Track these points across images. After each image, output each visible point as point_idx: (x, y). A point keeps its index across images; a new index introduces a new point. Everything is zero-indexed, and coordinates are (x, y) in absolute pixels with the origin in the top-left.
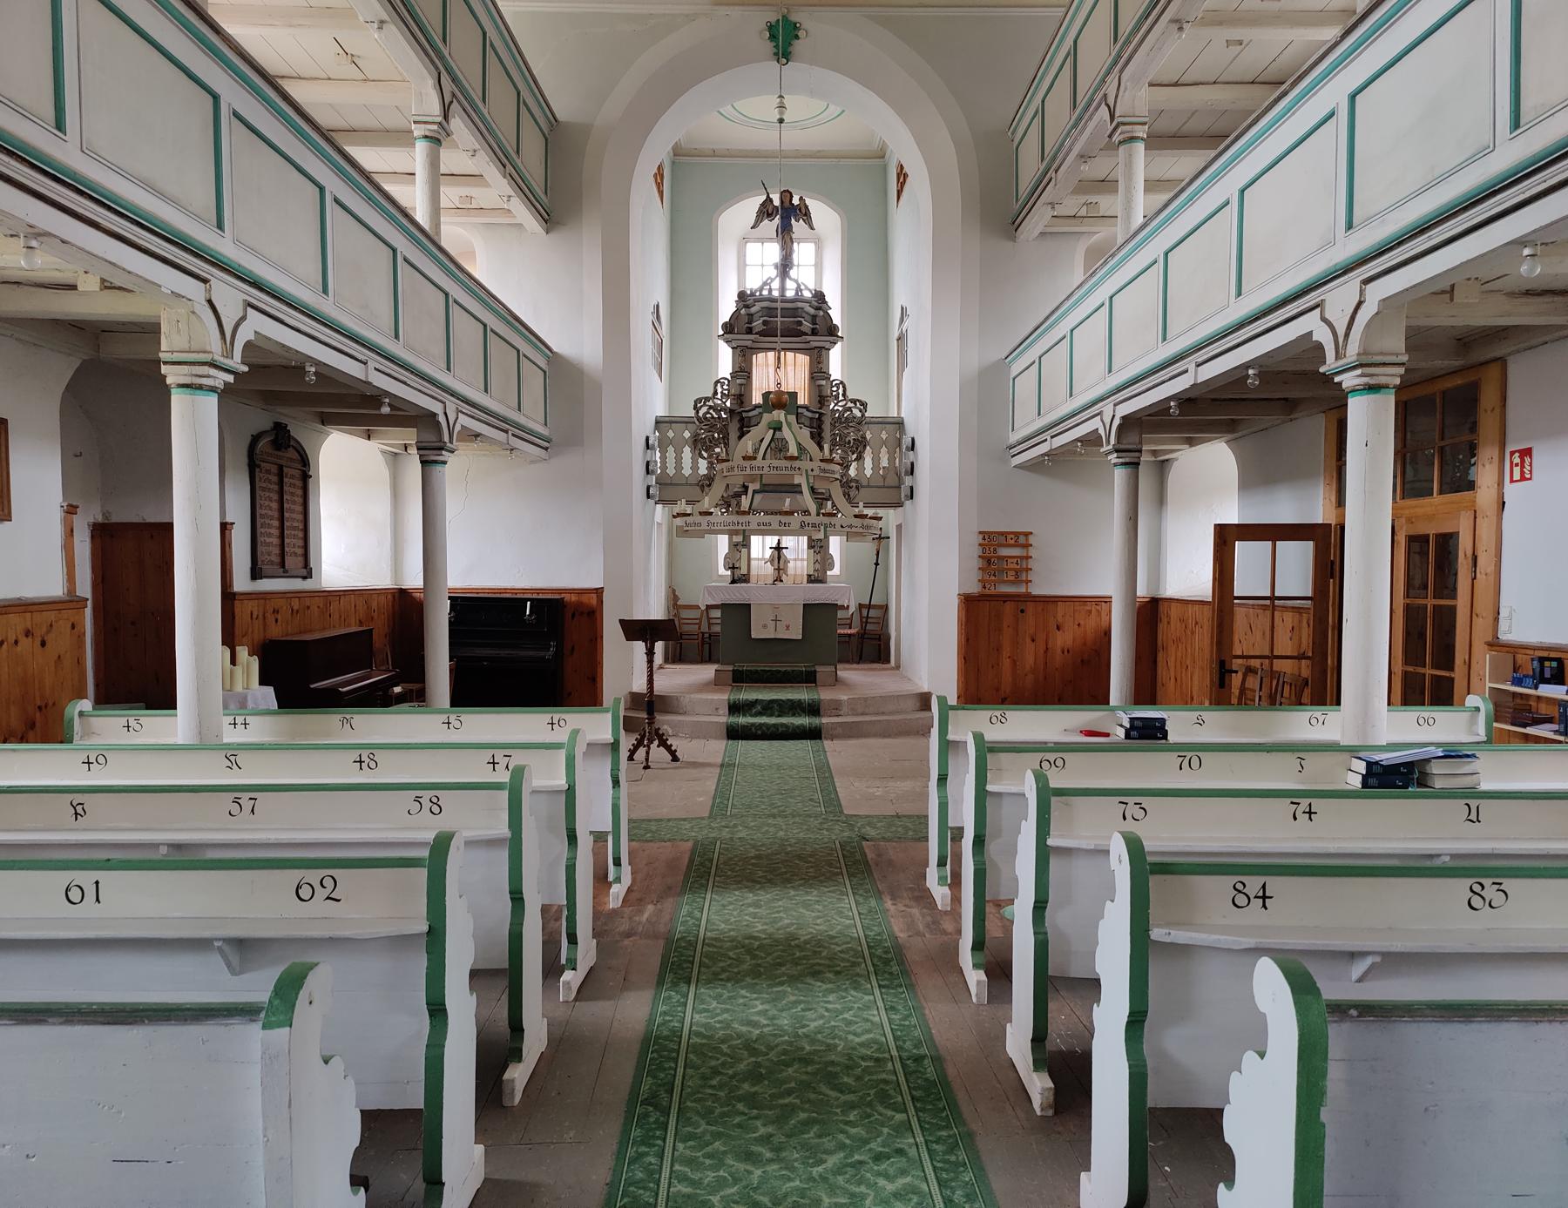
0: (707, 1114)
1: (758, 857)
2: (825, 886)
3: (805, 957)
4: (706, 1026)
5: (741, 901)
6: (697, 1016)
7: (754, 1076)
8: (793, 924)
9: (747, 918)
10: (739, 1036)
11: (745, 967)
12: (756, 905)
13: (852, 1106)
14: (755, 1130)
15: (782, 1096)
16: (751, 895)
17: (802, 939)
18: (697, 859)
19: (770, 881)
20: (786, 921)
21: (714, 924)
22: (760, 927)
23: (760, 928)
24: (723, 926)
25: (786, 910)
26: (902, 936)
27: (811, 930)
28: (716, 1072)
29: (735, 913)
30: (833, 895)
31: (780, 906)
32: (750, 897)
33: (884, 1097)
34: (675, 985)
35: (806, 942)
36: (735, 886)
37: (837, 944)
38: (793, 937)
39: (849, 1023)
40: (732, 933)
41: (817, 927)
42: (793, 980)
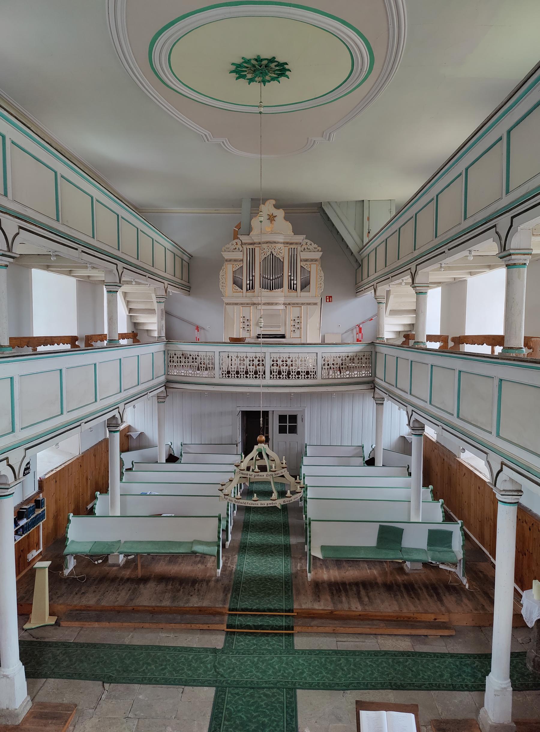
0: (278, 524)
1: (269, 594)
2: (250, 576)
3: (260, 550)
4: (279, 536)
5: (274, 570)
6: (281, 538)
7: (271, 529)
8: (262, 560)
9: (273, 563)
10: (274, 535)
11: (273, 548)
12: (270, 568)
13: (258, 525)
14: (270, 583)
15: (266, 564)
16: (272, 573)
17: (260, 555)
18: (290, 594)
19: (266, 580)
20: (263, 561)
21: (281, 561)
22: (269, 559)
23: (269, 559)
24: (278, 560)
25: (262, 566)
26: (236, 556)
27: (257, 558)
28: (277, 530)
29: (276, 565)
30: (248, 572)
31: (264, 567)
32: (272, 571)
33: (253, 526)
34: (287, 544)
35: (259, 554)
36: (277, 577)
37: (252, 553)
38: (262, 556)
39: (255, 536)
40: (276, 557)
41: (256, 559)
42: (263, 545)
